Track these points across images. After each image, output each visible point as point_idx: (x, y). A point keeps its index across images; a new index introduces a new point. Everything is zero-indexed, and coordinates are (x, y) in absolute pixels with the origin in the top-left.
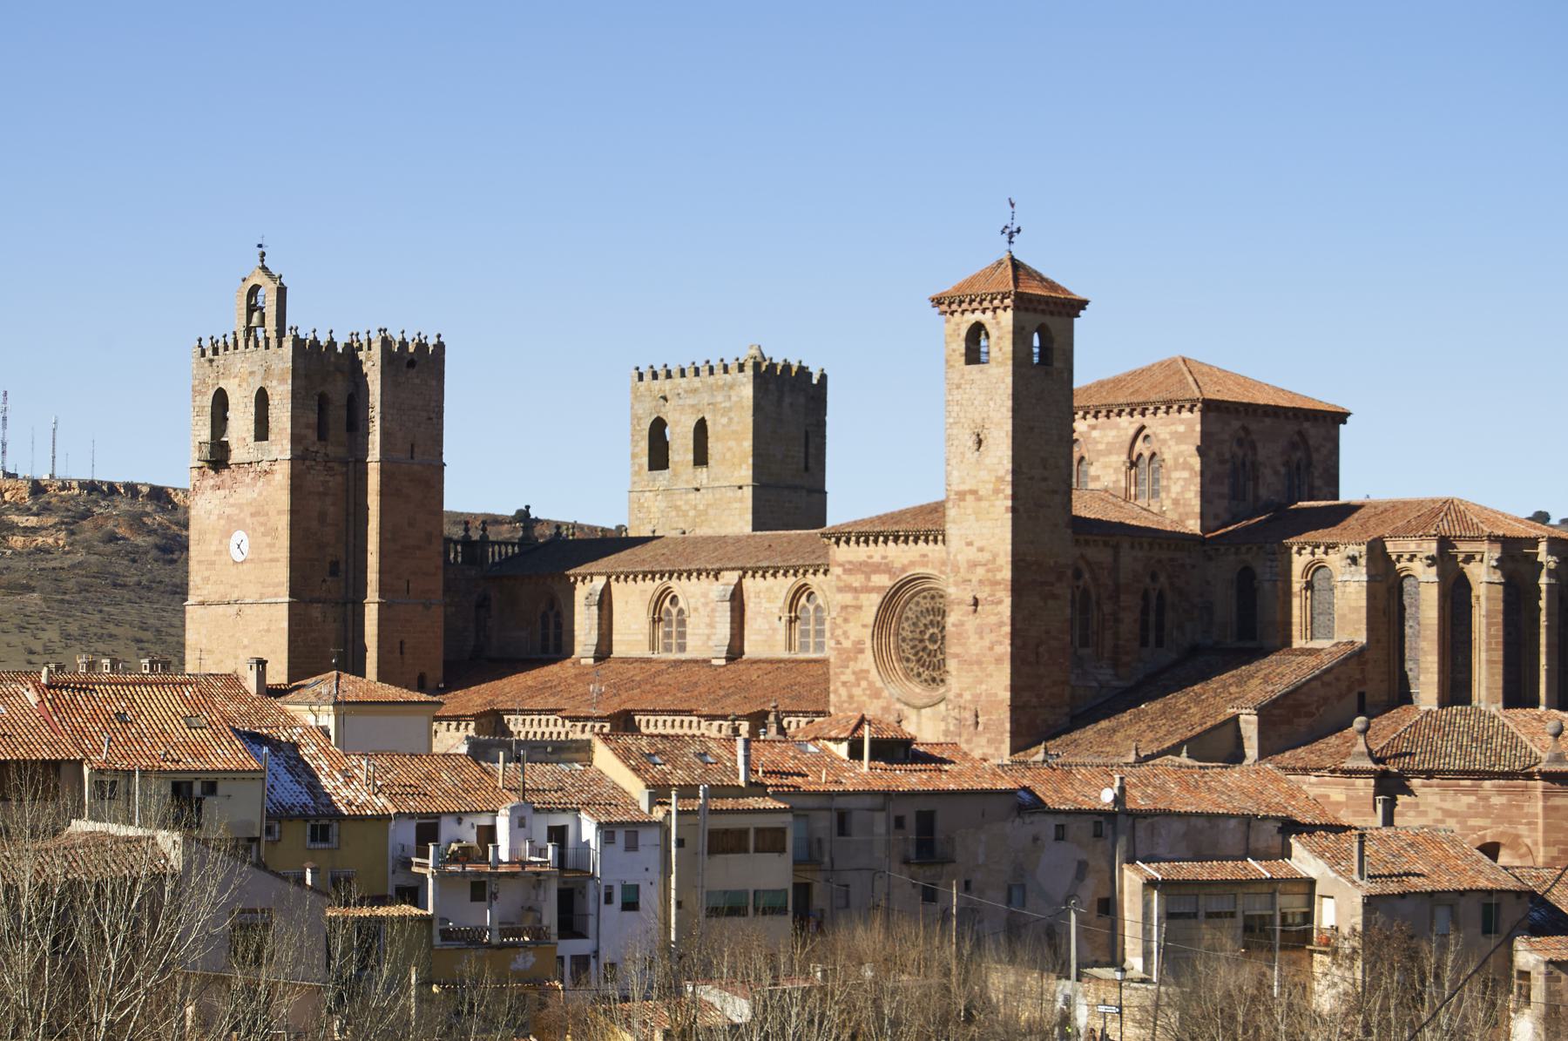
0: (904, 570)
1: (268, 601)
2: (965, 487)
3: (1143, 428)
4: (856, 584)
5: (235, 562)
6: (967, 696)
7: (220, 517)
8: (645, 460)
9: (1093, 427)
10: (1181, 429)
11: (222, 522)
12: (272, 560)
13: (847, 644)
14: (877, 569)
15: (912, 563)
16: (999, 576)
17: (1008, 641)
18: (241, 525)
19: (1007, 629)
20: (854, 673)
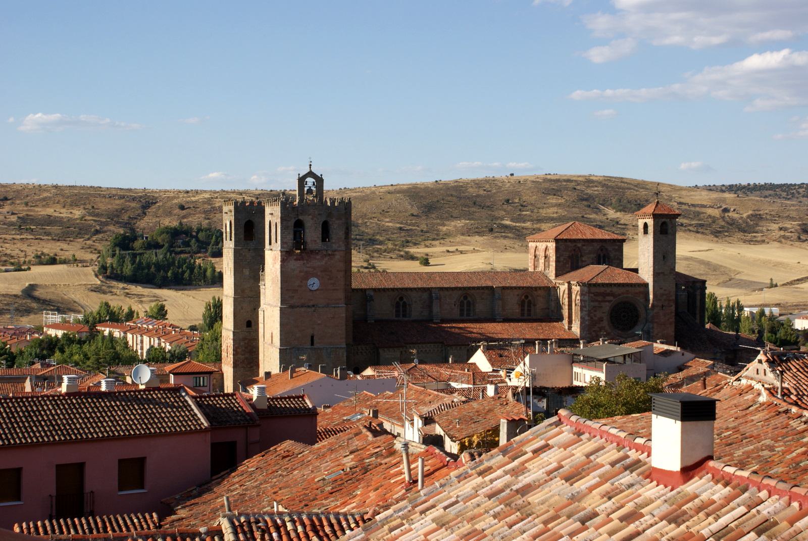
0: (619, 295)
1: (333, 306)
2: (660, 271)
3: (602, 246)
4: (599, 299)
5: (311, 290)
6: (660, 334)
7: (300, 272)
8: (242, 236)
9: (584, 245)
10: (617, 247)
11: (303, 274)
12: (334, 290)
13: (596, 318)
14: (608, 295)
15: (623, 293)
16: (671, 298)
17: (674, 318)
18: (317, 276)
19: (674, 314)
20: (599, 327)
